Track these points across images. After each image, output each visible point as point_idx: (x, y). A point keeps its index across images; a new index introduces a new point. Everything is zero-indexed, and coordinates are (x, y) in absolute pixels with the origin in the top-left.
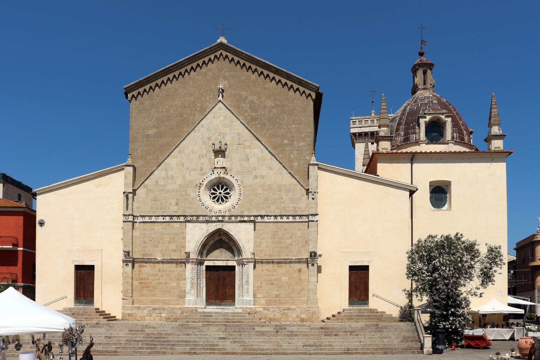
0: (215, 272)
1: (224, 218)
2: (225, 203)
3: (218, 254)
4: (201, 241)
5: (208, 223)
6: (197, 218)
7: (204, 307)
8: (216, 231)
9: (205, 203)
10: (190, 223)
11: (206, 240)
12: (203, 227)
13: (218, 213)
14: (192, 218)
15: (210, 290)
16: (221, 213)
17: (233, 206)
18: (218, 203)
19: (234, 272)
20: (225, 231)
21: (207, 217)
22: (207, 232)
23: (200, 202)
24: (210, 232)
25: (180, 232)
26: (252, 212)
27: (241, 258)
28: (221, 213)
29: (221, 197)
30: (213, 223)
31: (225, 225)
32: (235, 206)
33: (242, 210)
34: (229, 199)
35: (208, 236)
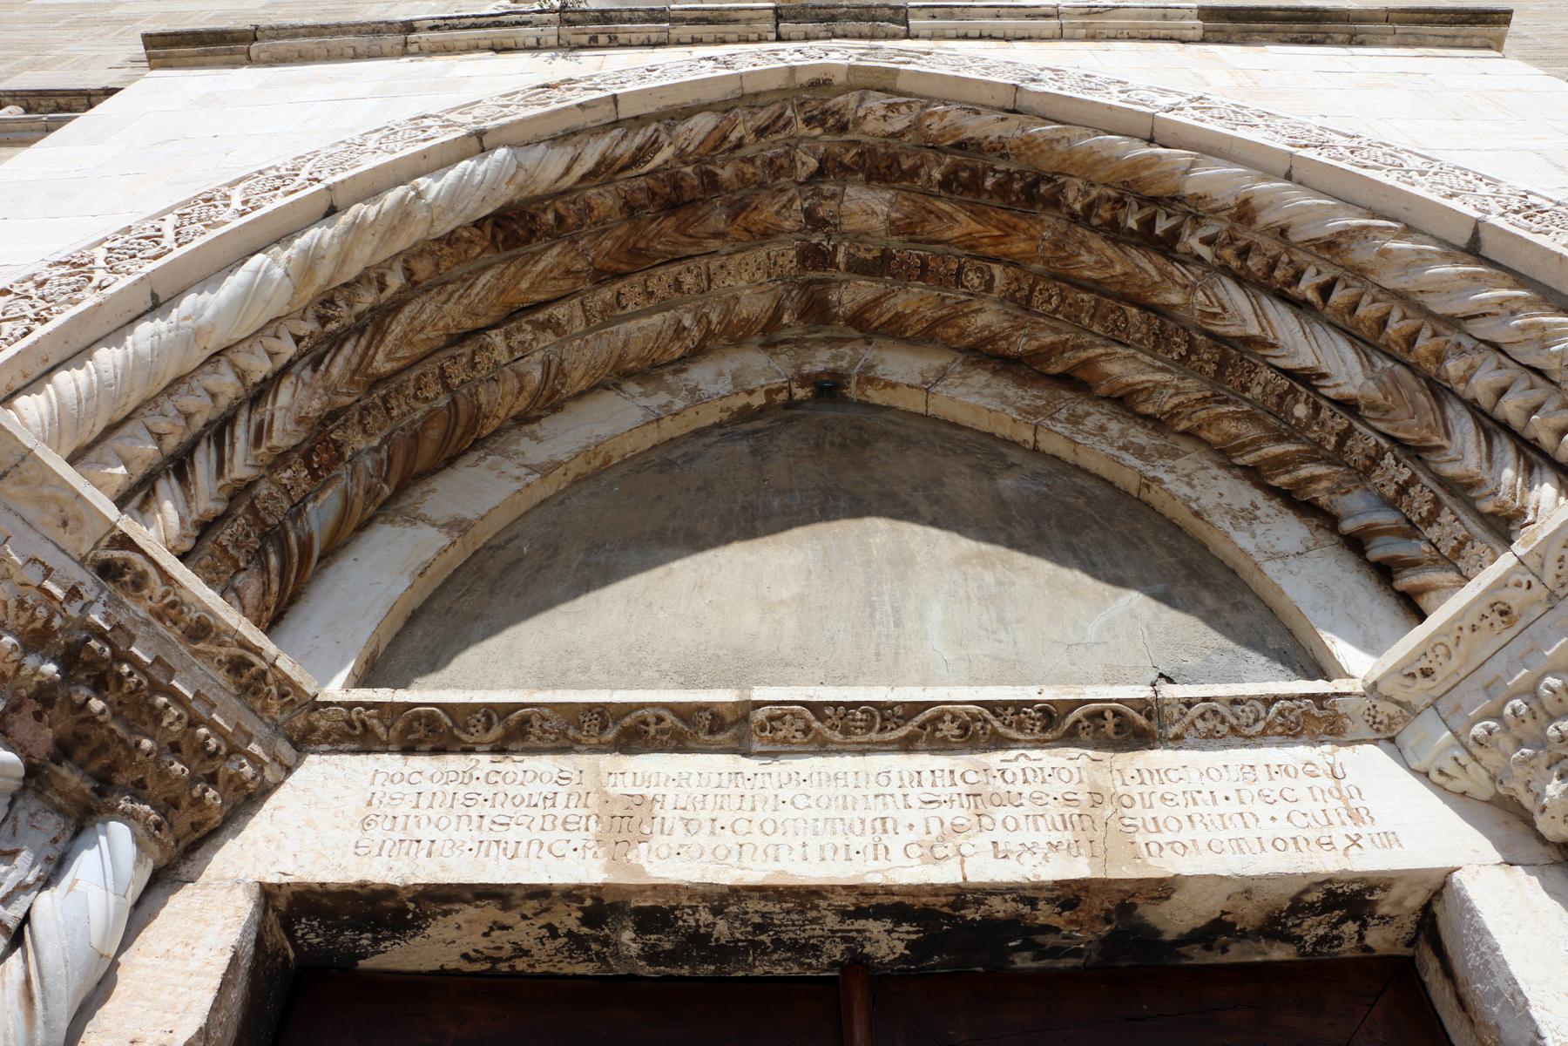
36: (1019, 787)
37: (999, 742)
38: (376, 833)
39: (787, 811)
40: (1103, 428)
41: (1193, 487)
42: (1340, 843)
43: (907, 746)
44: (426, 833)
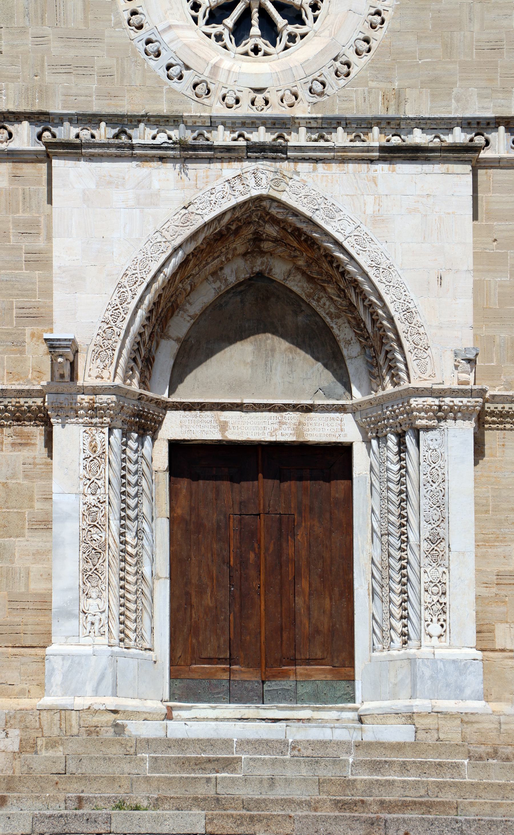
0: (225, 485)
1: (280, 137)
2: (286, 48)
3: (245, 372)
4: (148, 278)
5: (186, 160)
6: (117, 136)
7: (162, 708)
8: (238, 214)
9: (166, 37)
10: (78, 157)
11: (174, 275)
12: (156, 185)
13: (245, 102)
14: (85, 135)
15: (194, 600)
16: (267, 102)
17: (338, 64)
18: (241, 49)
19: (342, 484)
20: (296, 213)
21: (177, 127)
22: (184, 225)
23: (133, 34)
24: (200, 222)
25: (16, 224)
26: (458, 101)
27: (390, 389)
28: (267, 102)
29: (263, 12)
30: (221, 160)
31: (298, 173)
32: (353, 58)
33: (396, 85)
34: (309, 21)
35: (190, 248)
36: (287, 421)
37: (285, 411)
38: (184, 429)
39: (249, 425)
40: (325, 304)
41: (339, 330)
42: (337, 435)
43: (269, 411)
44: (192, 429)
